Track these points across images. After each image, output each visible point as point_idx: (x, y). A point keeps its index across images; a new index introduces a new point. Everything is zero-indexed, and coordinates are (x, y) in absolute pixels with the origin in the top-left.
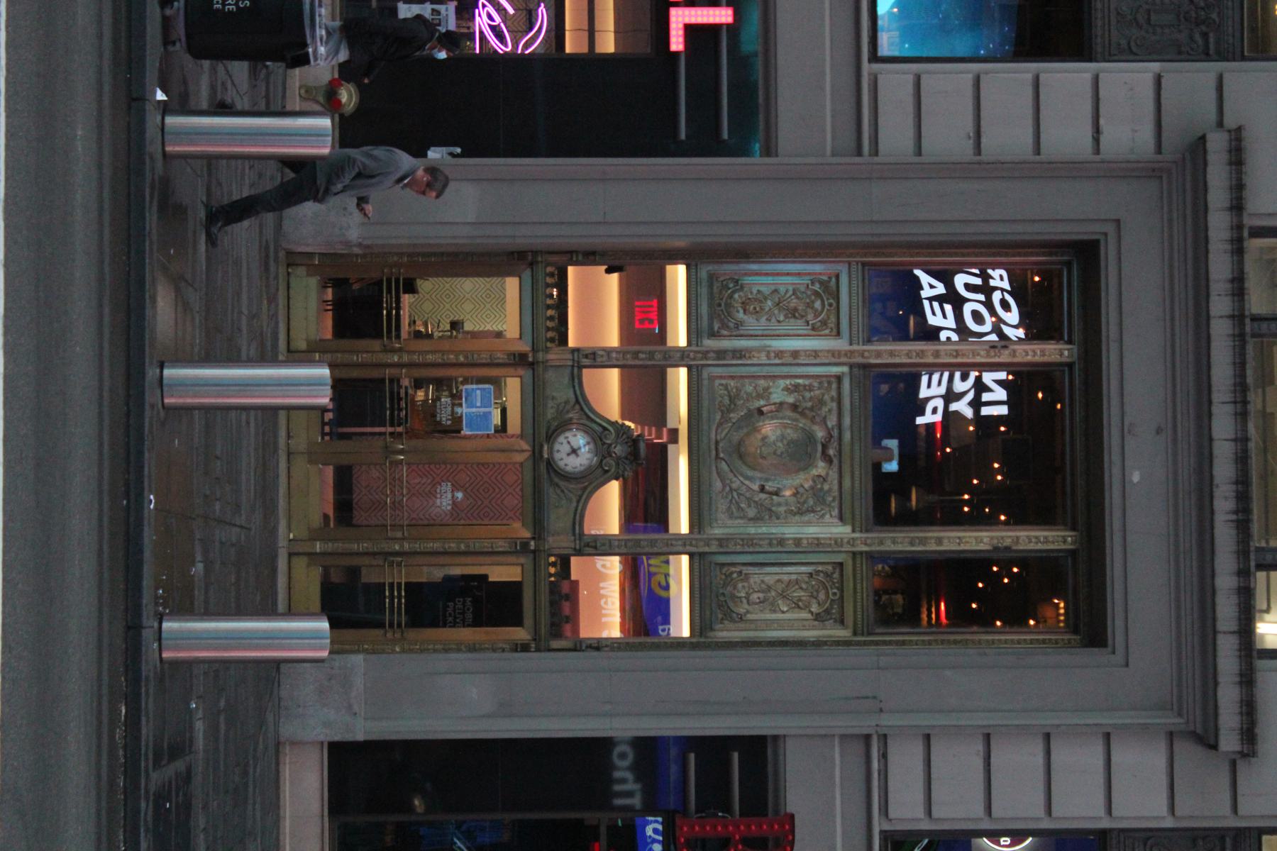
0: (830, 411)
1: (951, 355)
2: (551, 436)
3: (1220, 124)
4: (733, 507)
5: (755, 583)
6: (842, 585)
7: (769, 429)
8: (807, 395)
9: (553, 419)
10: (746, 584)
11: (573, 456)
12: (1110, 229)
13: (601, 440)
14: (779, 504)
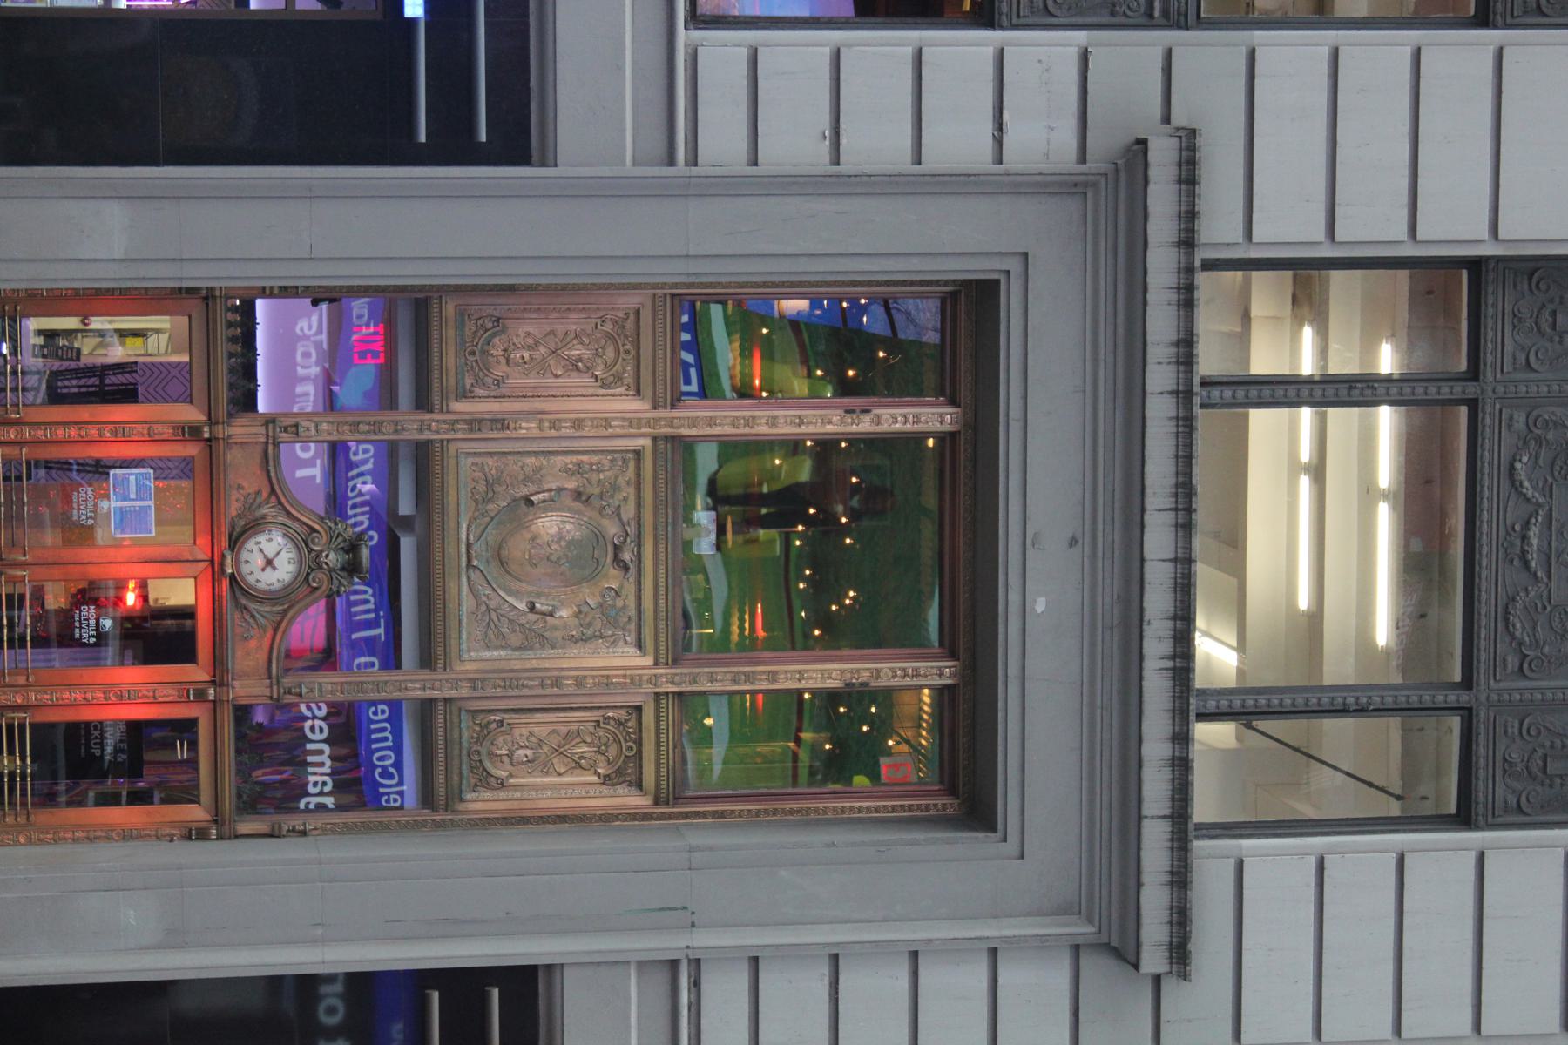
0: (625, 499)
1: (792, 423)
2: (235, 542)
4: (490, 633)
5: (521, 735)
6: (641, 738)
7: (548, 525)
8: (594, 477)
9: (239, 516)
10: (509, 738)
11: (269, 569)
12: (1014, 265)
13: (307, 546)
14: (555, 628)
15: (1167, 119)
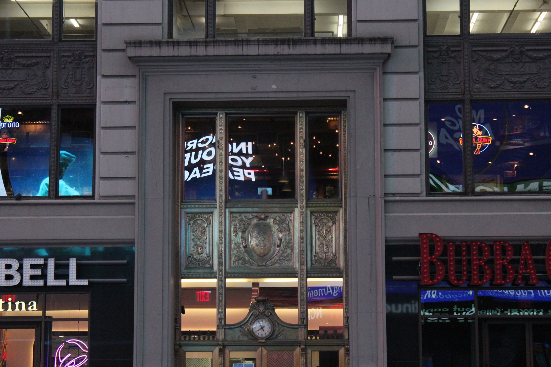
0: (245, 217)
1: (221, 165)
3: (124, 50)
4: (286, 259)
5: (319, 249)
6: (321, 212)
7: (253, 242)
8: (238, 227)
9: (248, 337)
10: (320, 253)
11: (264, 329)
12: (168, 97)
13: (257, 316)
14: (286, 239)
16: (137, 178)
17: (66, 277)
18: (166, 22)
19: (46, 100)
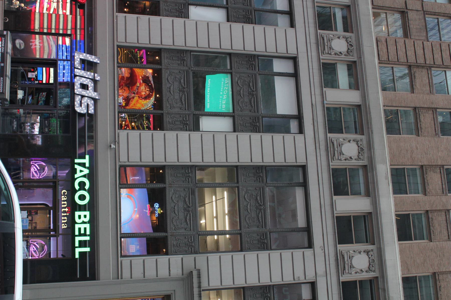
12: (173, 292)
15: (195, 268)
16: (131, 279)
17: (80, 246)
18: (210, 288)
19: (170, 230)
